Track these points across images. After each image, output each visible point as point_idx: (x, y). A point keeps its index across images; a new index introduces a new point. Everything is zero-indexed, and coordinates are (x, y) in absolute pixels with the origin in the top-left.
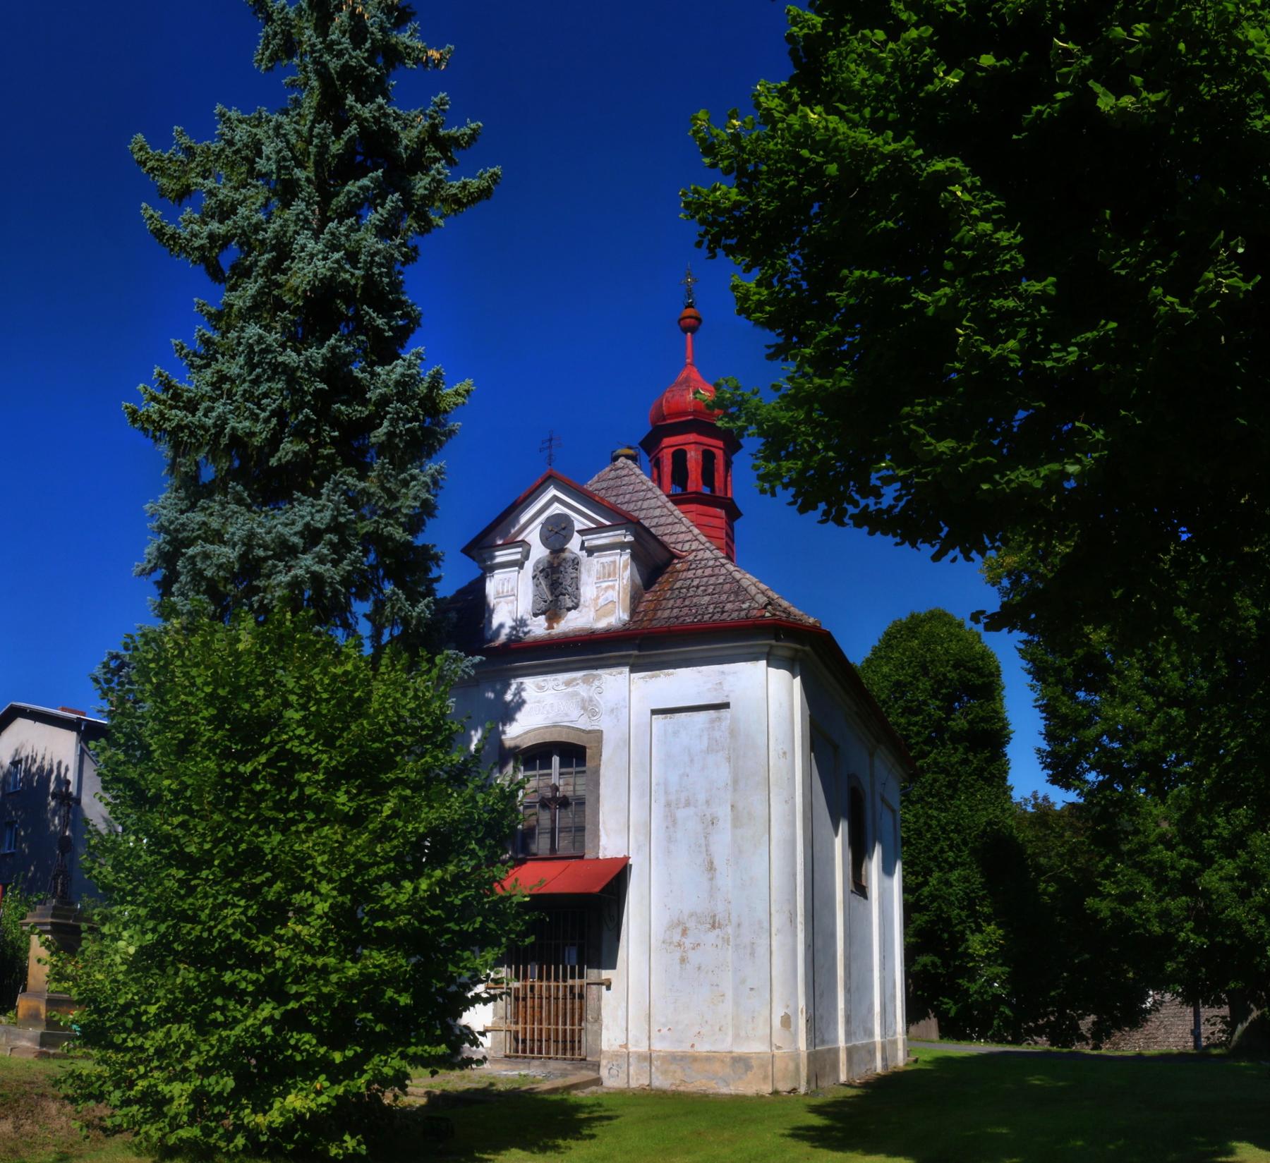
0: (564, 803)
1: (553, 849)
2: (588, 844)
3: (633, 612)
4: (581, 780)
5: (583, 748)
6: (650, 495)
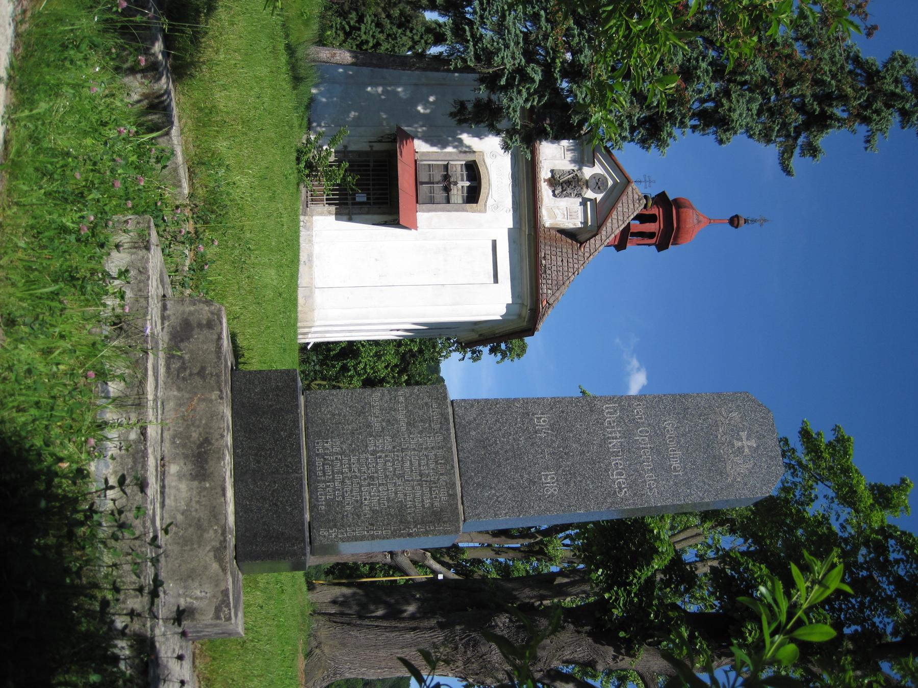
0: (447, 189)
1: (422, 183)
2: (424, 206)
3: (549, 229)
4: (460, 201)
5: (476, 202)
6: (620, 223)
